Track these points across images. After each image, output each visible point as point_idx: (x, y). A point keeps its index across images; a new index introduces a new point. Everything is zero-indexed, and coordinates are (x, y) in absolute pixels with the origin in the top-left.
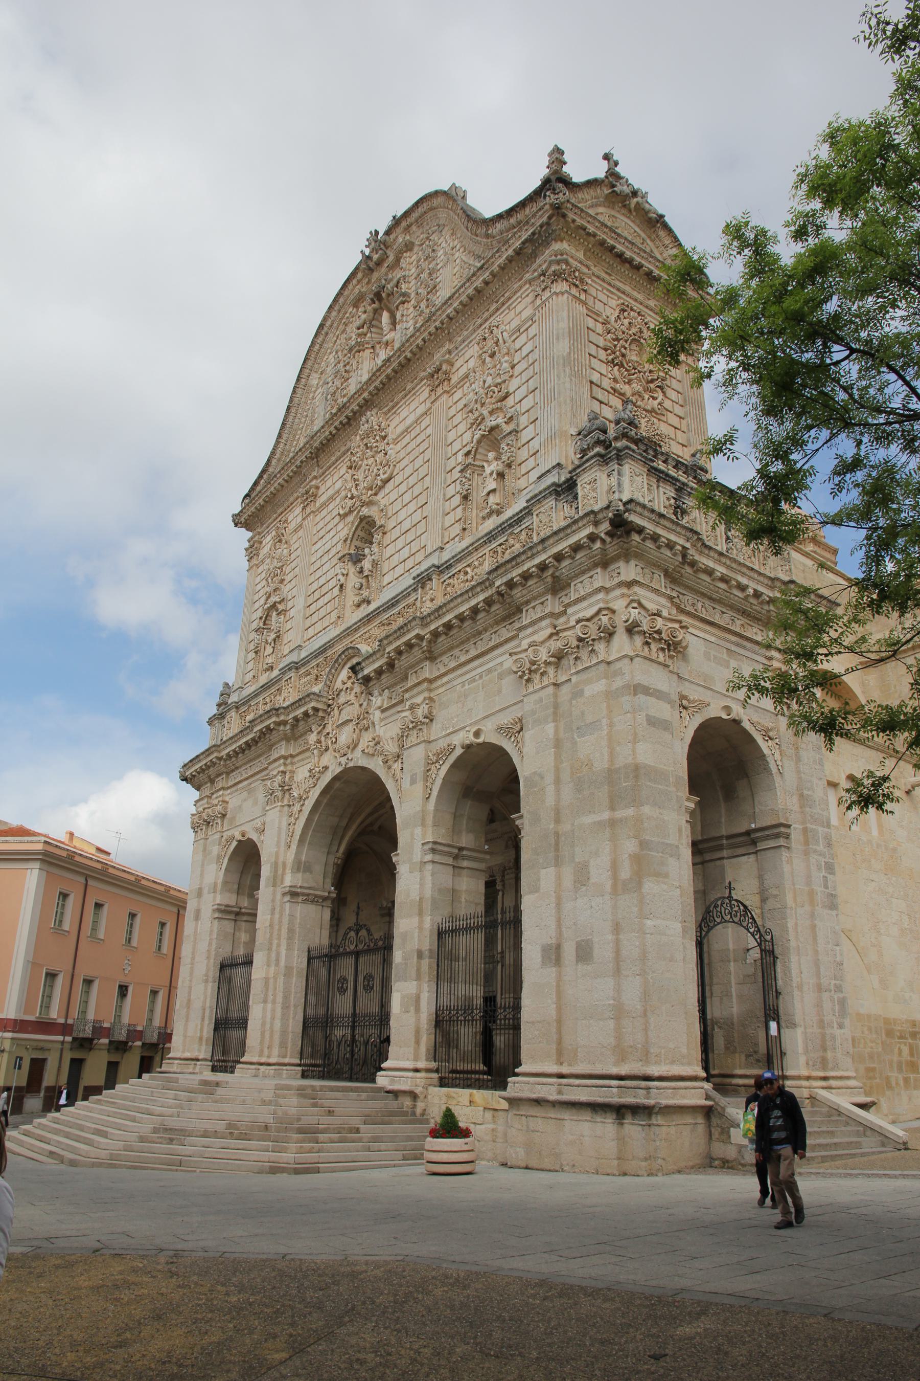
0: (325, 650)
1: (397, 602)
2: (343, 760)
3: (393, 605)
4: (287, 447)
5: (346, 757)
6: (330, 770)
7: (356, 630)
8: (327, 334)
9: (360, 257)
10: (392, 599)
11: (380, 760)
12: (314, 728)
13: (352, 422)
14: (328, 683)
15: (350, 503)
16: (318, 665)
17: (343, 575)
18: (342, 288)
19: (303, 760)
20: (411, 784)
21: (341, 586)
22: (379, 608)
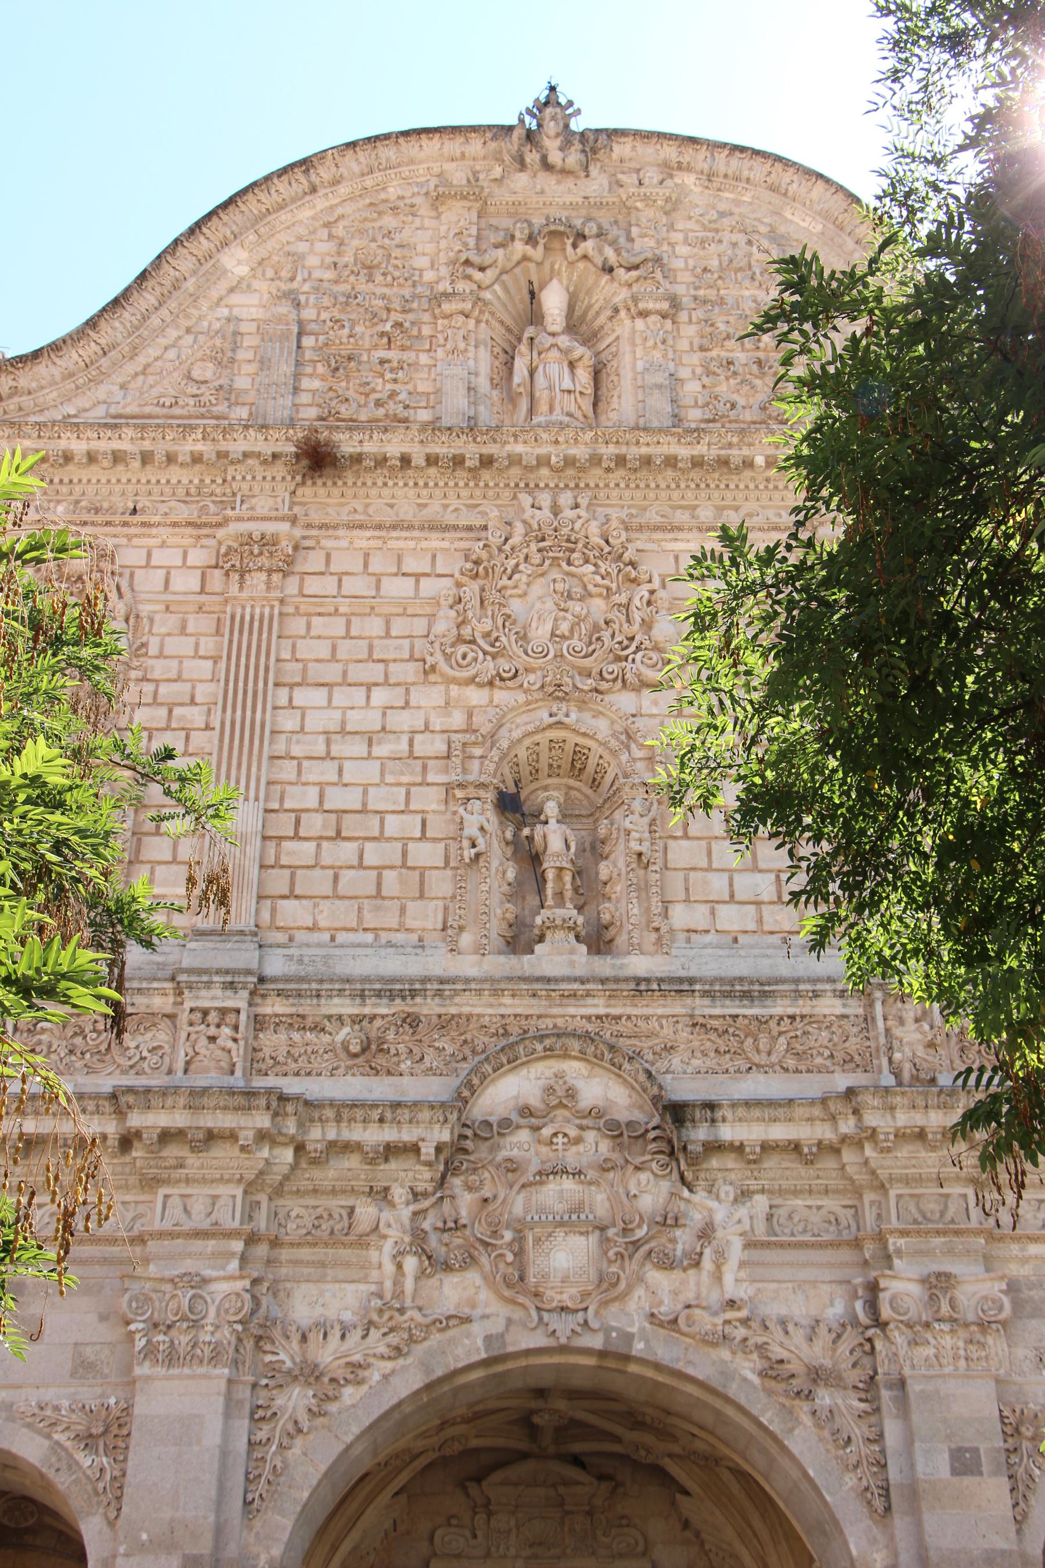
0: (413, 993)
1: (764, 995)
2: (555, 1322)
3: (746, 995)
4: (104, 362)
5: (572, 1322)
6: (478, 1331)
7: (574, 995)
8: (314, 190)
9: (514, 121)
10: (752, 983)
11: (748, 1368)
12: (399, 1193)
13: (486, 475)
14: (466, 1093)
15: (489, 667)
16: (357, 1020)
17: (482, 829)
18: (406, 134)
19: (323, 1264)
20: (955, 1472)
21: (478, 855)
22: (691, 981)
